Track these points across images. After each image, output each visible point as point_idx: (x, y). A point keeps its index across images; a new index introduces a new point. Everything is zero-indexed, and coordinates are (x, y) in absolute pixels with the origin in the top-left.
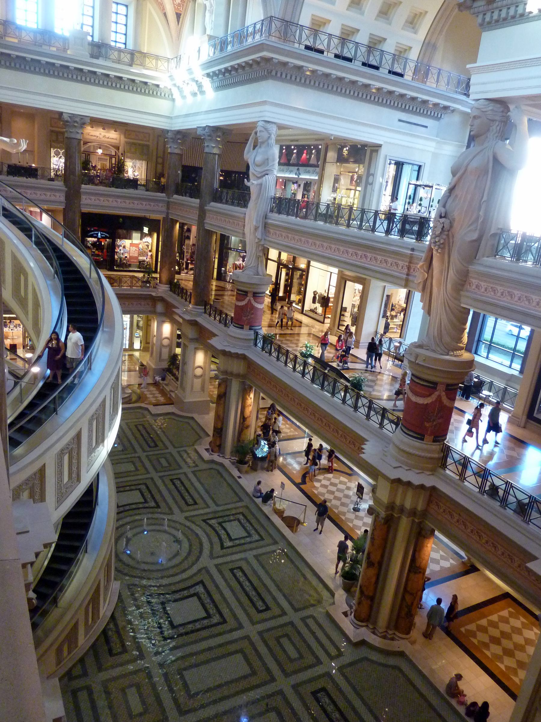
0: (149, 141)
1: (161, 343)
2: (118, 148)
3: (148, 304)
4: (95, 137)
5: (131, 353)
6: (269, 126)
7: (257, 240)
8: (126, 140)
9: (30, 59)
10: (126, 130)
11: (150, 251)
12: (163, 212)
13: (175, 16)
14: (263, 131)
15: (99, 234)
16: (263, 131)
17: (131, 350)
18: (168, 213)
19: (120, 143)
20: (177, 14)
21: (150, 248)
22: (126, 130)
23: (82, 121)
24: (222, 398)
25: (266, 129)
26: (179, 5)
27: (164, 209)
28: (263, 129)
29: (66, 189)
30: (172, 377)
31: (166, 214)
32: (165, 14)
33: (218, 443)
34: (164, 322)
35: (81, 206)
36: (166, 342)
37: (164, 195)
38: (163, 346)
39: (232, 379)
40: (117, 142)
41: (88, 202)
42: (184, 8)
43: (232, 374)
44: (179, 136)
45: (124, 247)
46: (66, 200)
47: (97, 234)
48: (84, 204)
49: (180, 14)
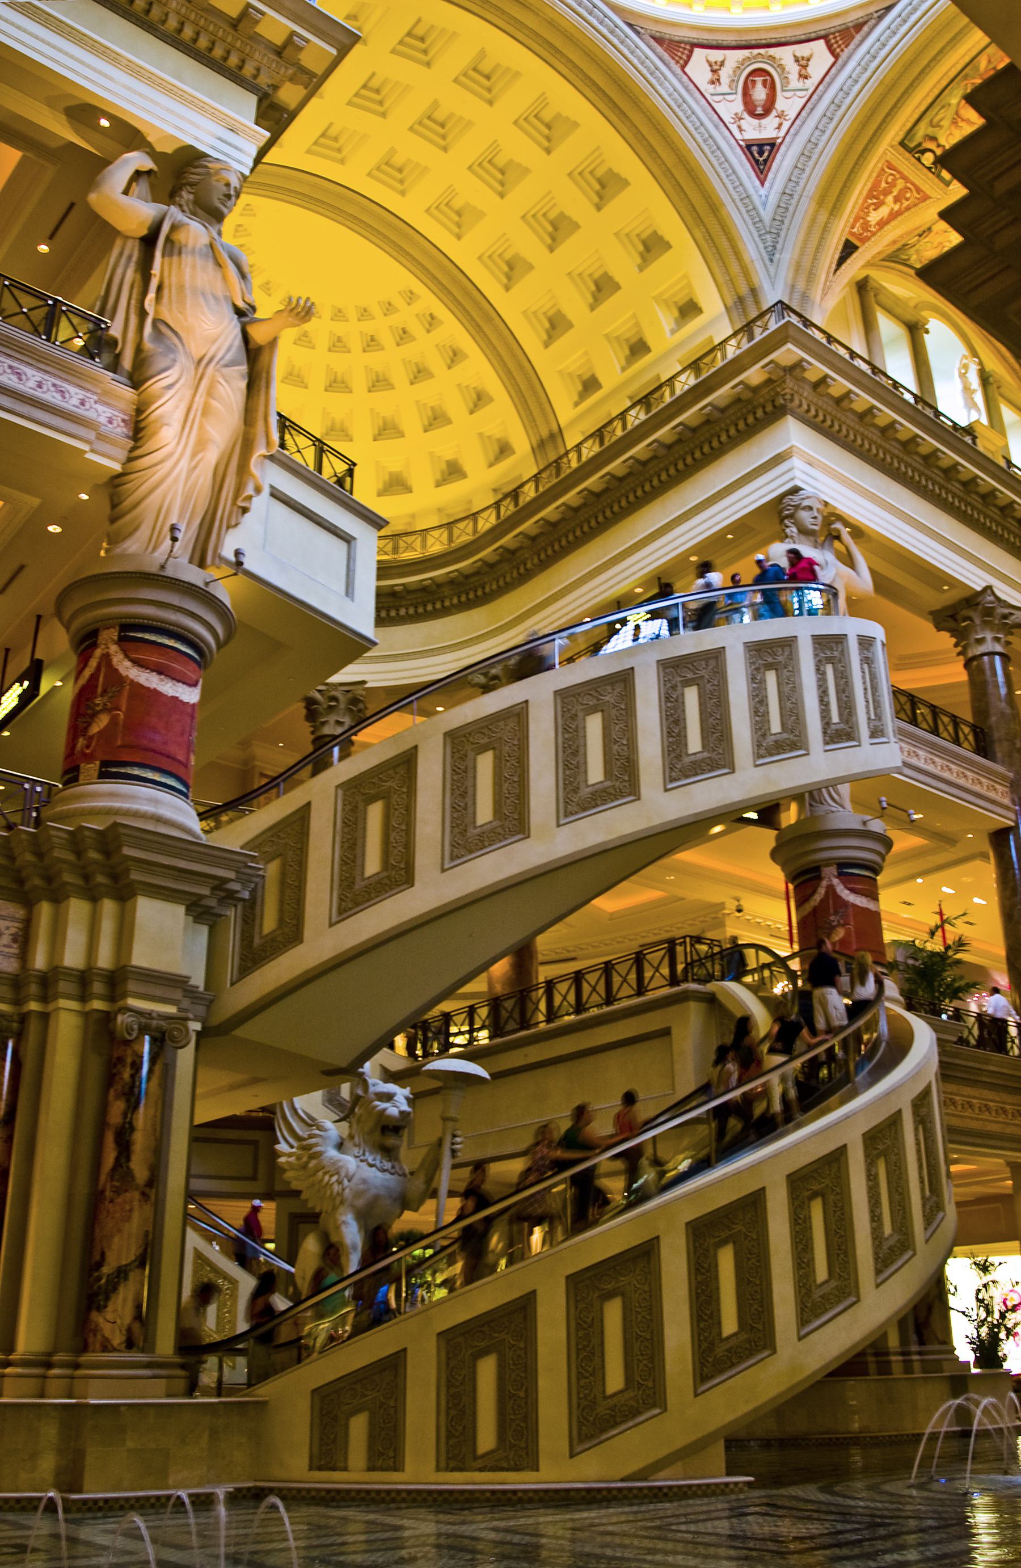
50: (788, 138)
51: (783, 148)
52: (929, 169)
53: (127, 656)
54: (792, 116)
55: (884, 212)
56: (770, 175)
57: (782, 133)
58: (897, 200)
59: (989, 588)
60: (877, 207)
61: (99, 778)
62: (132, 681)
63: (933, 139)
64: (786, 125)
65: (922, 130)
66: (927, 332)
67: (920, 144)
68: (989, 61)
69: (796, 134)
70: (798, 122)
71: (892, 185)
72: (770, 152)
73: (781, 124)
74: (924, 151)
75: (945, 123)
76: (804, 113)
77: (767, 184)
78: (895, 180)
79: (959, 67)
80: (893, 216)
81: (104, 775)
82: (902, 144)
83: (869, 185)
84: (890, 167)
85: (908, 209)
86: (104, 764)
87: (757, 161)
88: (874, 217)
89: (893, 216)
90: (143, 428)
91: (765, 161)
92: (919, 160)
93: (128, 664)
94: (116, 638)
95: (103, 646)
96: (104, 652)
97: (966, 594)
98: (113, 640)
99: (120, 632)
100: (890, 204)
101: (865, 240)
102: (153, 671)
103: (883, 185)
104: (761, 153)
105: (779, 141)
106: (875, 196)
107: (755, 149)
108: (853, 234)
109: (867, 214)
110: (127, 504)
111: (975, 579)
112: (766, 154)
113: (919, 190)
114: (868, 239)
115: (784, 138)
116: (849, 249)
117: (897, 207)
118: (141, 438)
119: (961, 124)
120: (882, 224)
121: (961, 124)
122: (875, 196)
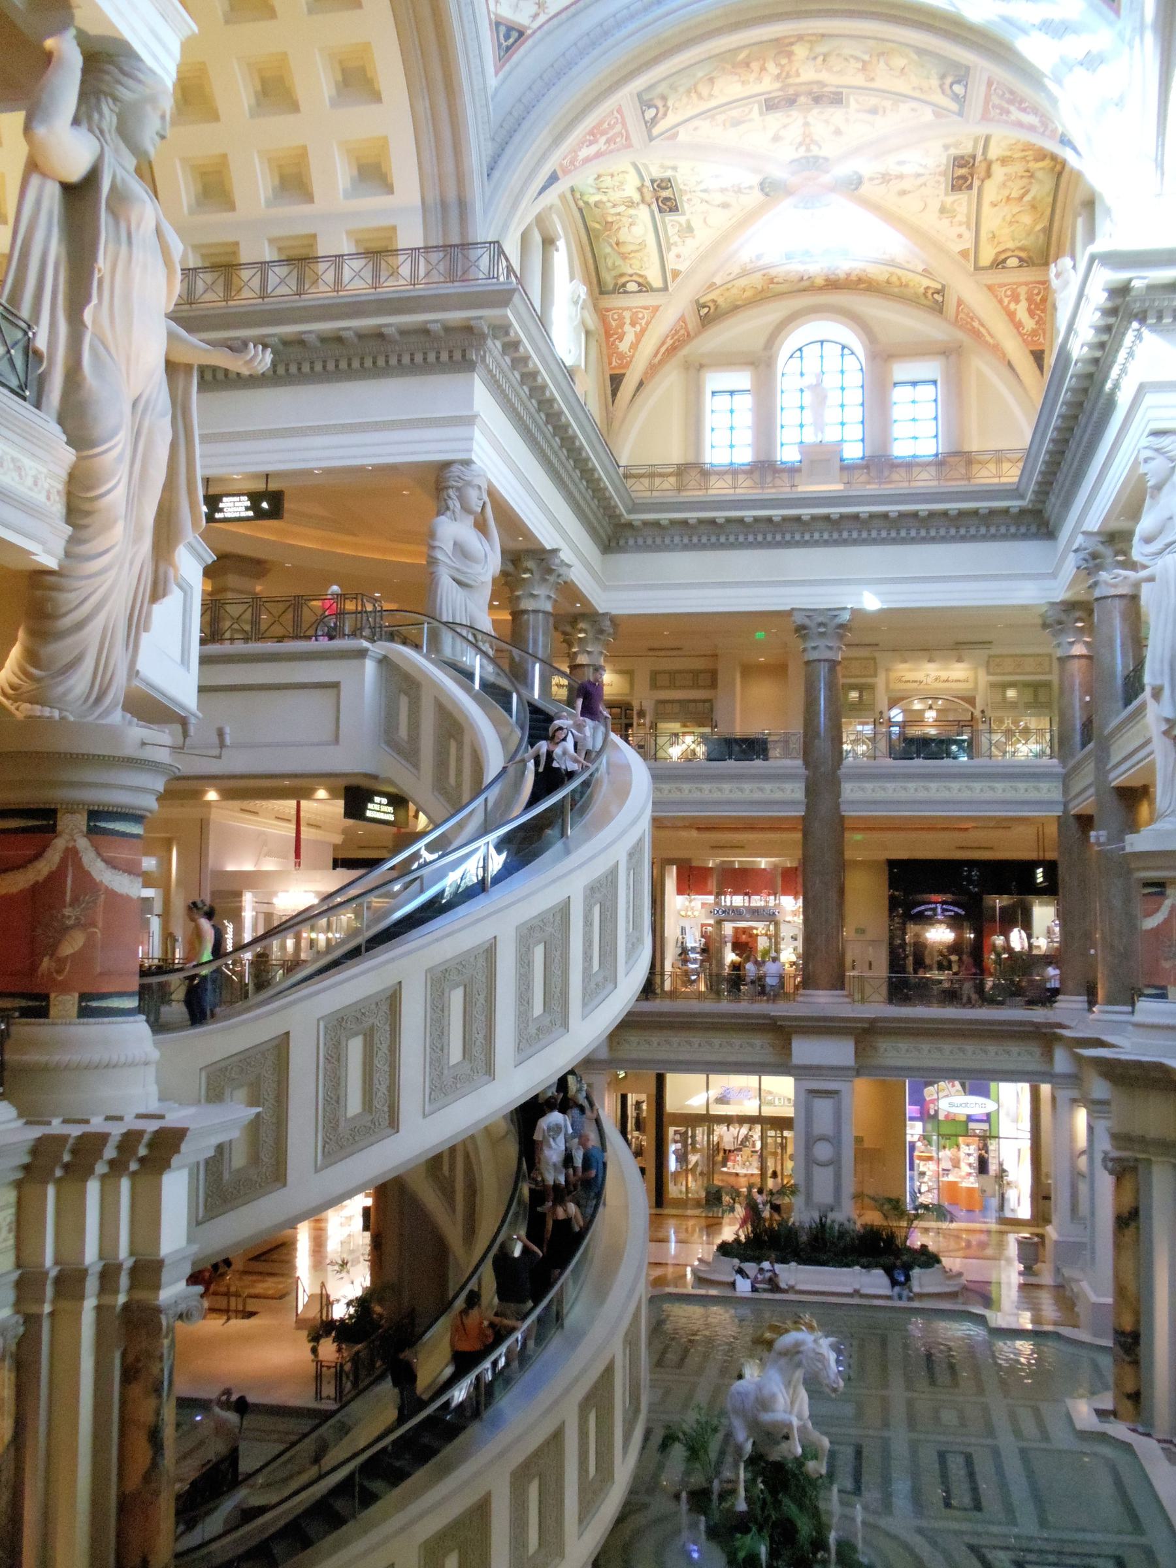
0: (1050, 672)
2: (971, 701)
4: (915, 685)
6: (1164, 441)
7: (1164, 727)
8: (992, 678)
9: (722, 521)
10: (990, 657)
12: (1057, 802)
13: (1031, 358)
14: (1153, 459)
15: (939, 910)
16: (1153, 459)
18: (1066, 804)
19: (976, 689)
20: (1033, 353)
22: (990, 657)
24: (1127, 1225)
25: (1157, 450)
26: (1034, 333)
27: (1057, 795)
28: (1148, 453)
31: (1061, 808)
32: (1010, 365)
33: (1130, 1387)
35: (842, 807)
37: (1055, 761)
39: (1149, 1161)
40: (970, 685)
41: (858, 796)
42: (1048, 335)
43: (1142, 1142)
46: (807, 796)
48: (852, 802)
49: (1042, 352)
50: (538, 34)
51: (529, 43)
52: (646, 123)
53: (99, 854)
54: (552, 13)
55: (593, 149)
56: (507, 67)
57: (535, 25)
58: (608, 141)
59: (555, 551)
60: (591, 143)
61: (79, 1017)
62: (107, 888)
63: (664, 98)
64: (542, 18)
65: (661, 88)
66: (557, 250)
67: (651, 100)
68: (748, 56)
69: (549, 33)
70: (555, 21)
71: (611, 127)
72: (515, 41)
73: (536, 16)
74: (649, 108)
75: (681, 89)
76: (564, 16)
77: (501, 75)
78: (616, 123)
79: (723, 49)
80: (598, 155)
81: (85, 1012)
82: (639, 95)
83: (594, 124)
84: (619, 111)
85: (611, 152)
86: (83, 997)
87: (500, 45)
88: (585, 152)
89: (598, 155)
90: (88, 514)
91: (508, 48)
92: (643, 113)
93: (100, 864)
94: (85, 829)
95: (66, 837)
96: (71, 845)
97: (530, 546)
98: (82, 832)
99: (89, 819)
100: (601, 144)
101: (566, 172)
102: (125, 871)
103: (606, 125)
104: (507, 37)
105: (529, 32)
106: (594, 133)
107: (503, 29)
108: (561, 165)
109: (580, 149)
110: (67, 622)
111: (547, 538)
112: (511, 40)
113: (628, 138)
114: (570, 171)
115: (534, 32)
116: (553, 178)
117: (604, 148)
118: (86, 527)
119: (693, 95)
120: (587, 160)
121: (693, 95)
122: (594, 133)
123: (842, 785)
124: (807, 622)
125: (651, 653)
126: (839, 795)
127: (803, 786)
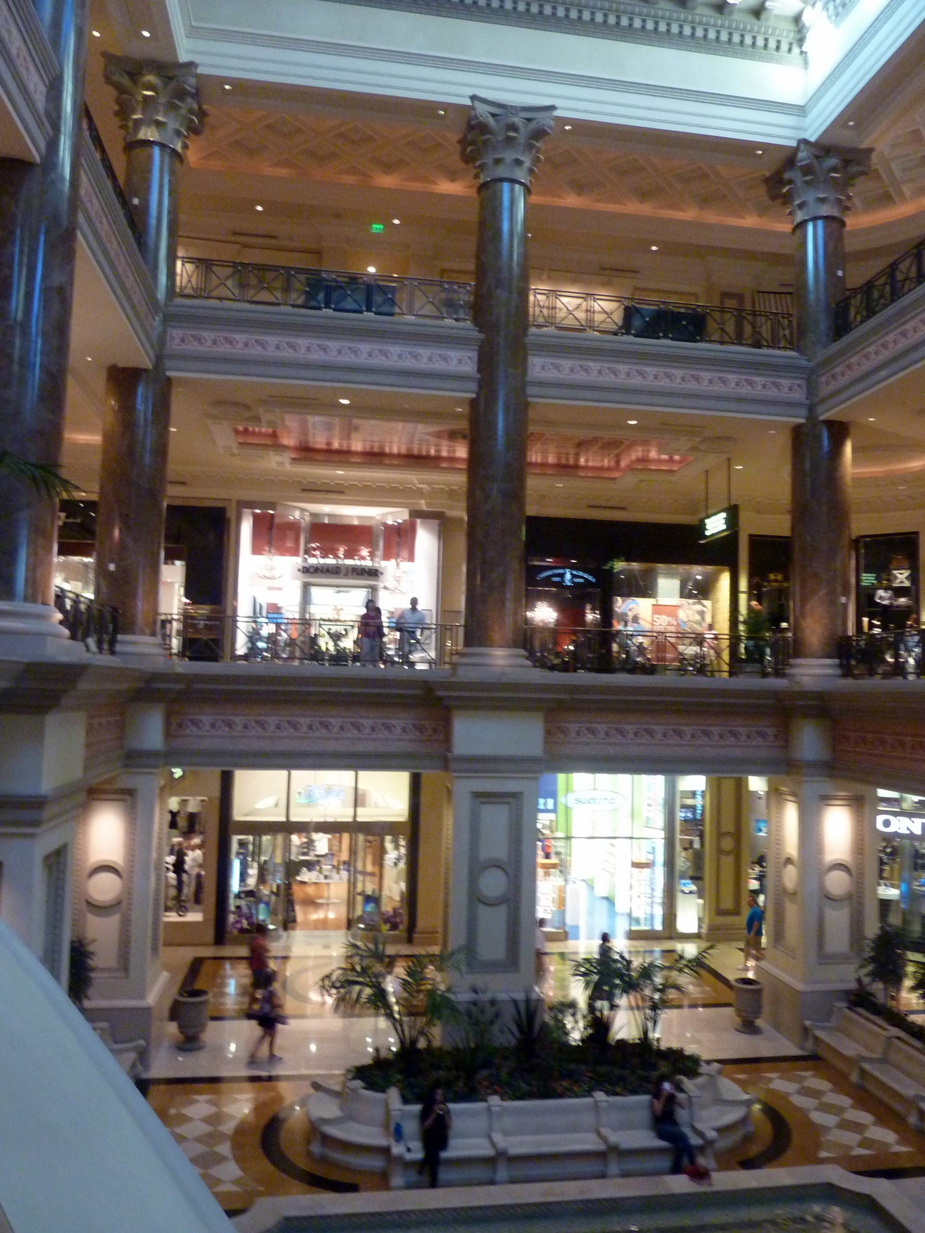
1: (822, 887)
3: (761, 734)
5: (668, 945)
11: (711, 627)
12: (799, 405)
17: (670, 938)
21: (708, 620)
23: (533, 125)
27: (799, 395)
29: (482, 336)
30: (895, 1031)
31: (804, 412)
34: (826, 799)
35: (530, 390)
36: (837, 883)
38: (829, 897)
44: (833, 161)
45: (636, 619)
47: (562, 576)
48: (541, 384)
123: (530, 358)
124: (491, 121)
125: (233, 238)
126: (524, 373)
127: (474, 355)
